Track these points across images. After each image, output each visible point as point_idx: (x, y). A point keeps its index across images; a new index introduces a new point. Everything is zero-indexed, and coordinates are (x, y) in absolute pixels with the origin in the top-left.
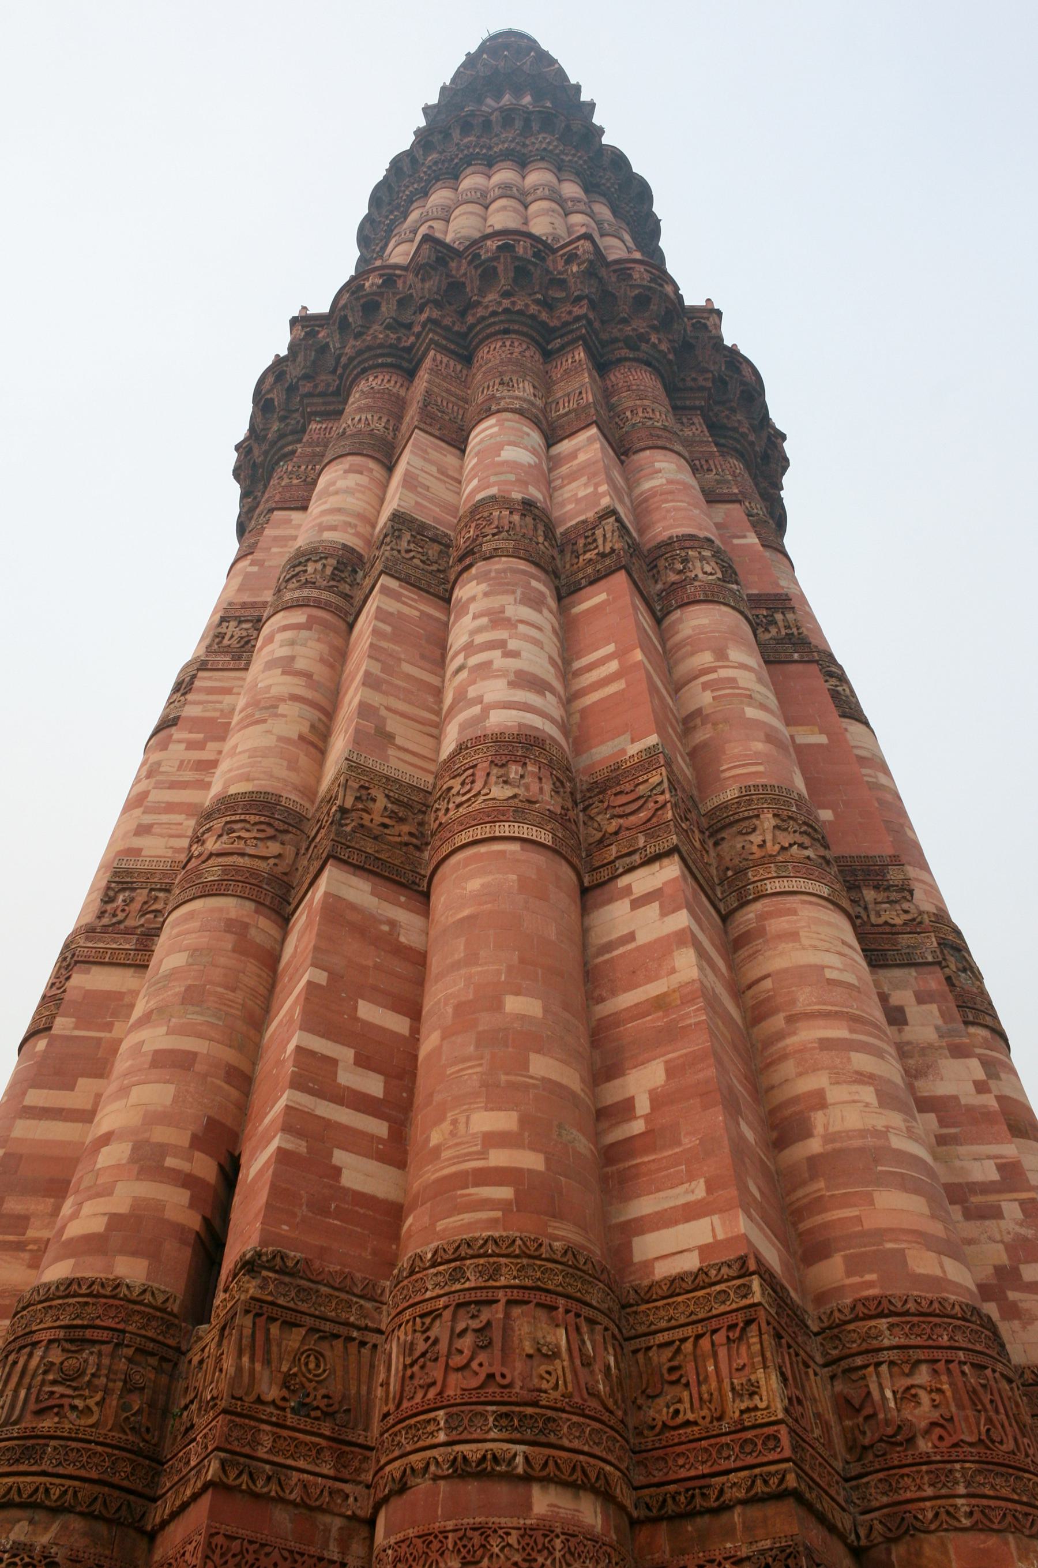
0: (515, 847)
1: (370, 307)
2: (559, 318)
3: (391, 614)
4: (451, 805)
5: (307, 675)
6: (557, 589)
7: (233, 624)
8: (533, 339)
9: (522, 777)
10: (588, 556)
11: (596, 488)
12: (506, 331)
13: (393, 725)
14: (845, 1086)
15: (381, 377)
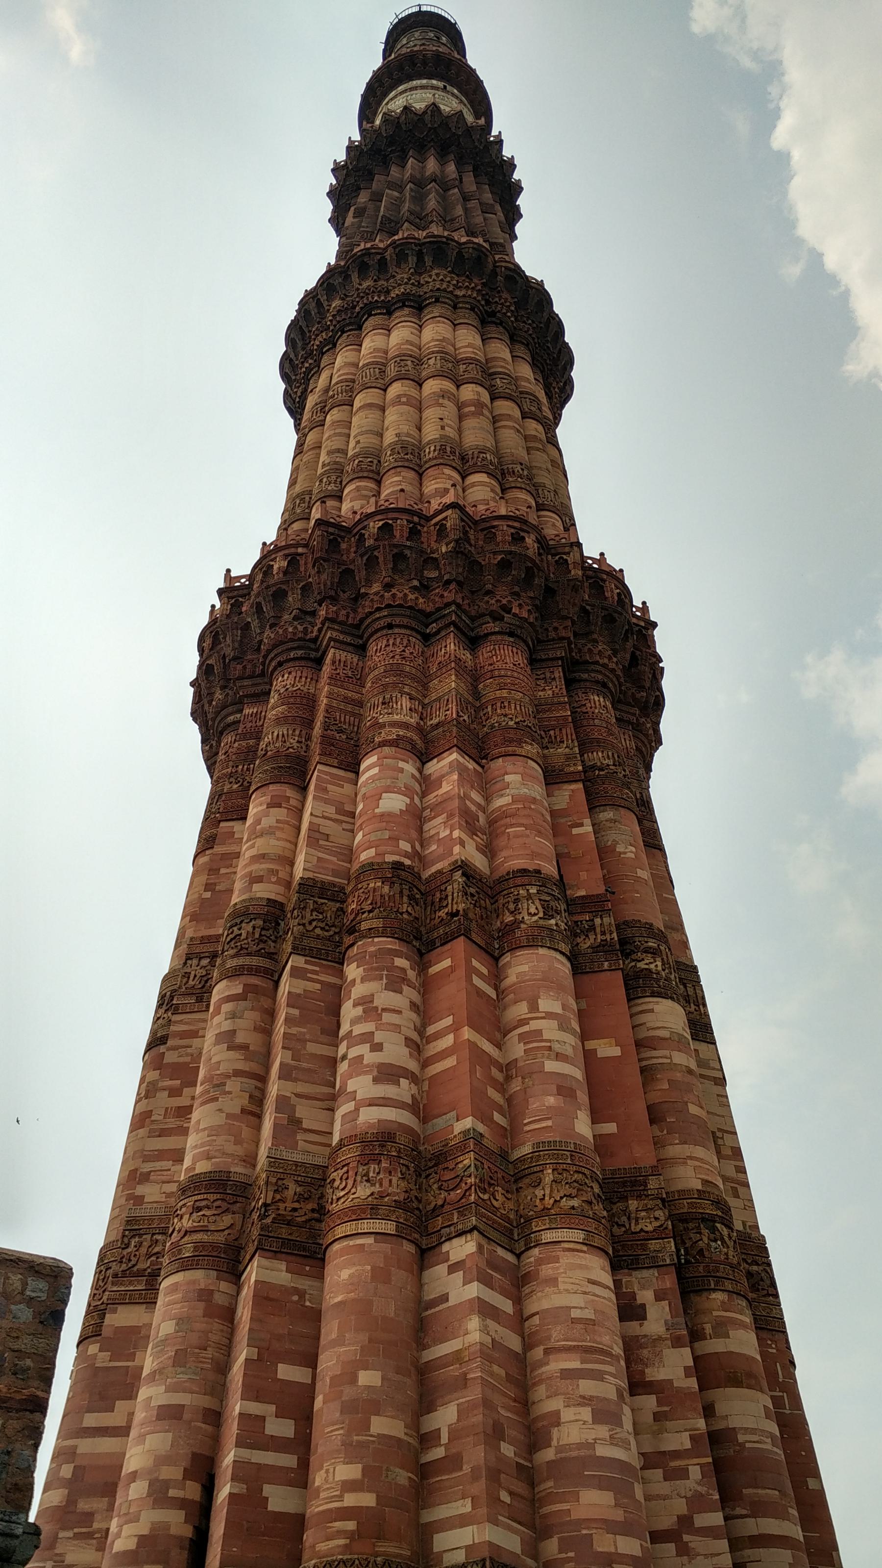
1: (279, 596)
2: (434, 602)
3: (299, 995)
4: (334, 1197)
6: (419, 950)
8: (412, 629)
9: (378, 1173)
11: (451, 832)
12: (390, 626)
13: (303, 1111)
14: (572, 1408)
15: (294, 674)
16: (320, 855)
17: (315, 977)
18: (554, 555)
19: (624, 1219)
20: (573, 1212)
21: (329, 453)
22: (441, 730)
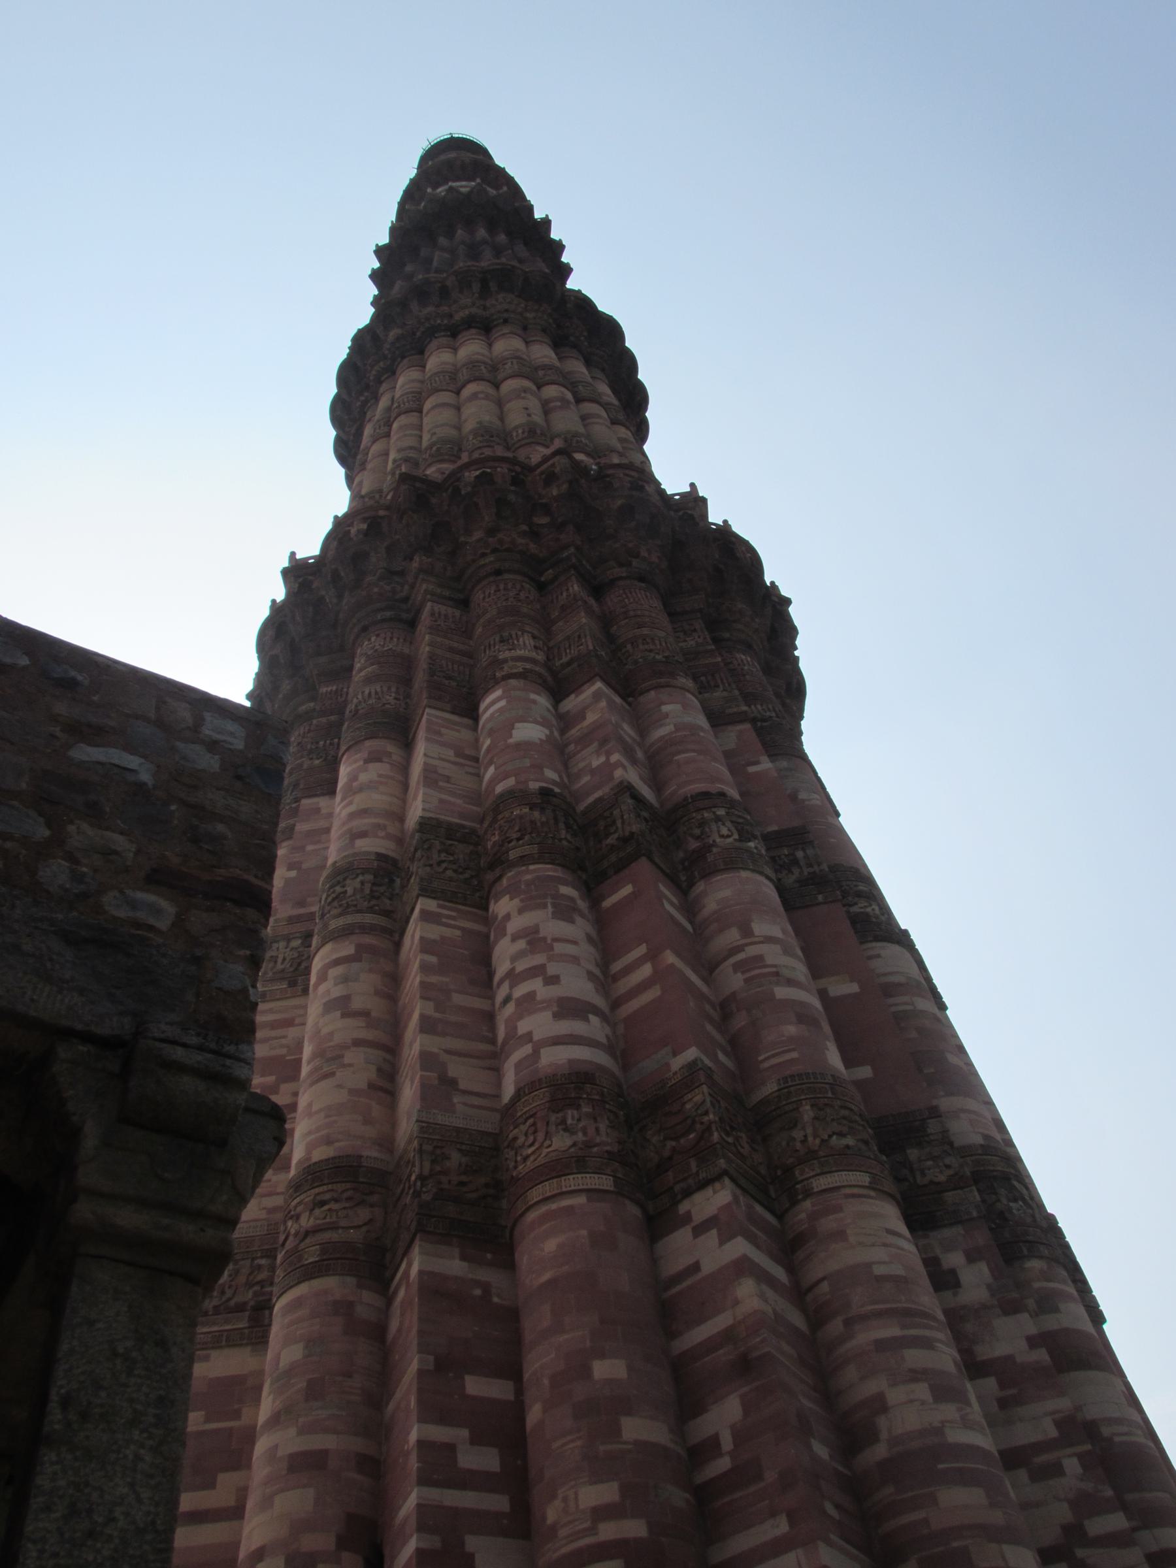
0: (581, 1200)
3: (434, 941)
4: (519, 1158)
5: (365, 1014)
9: (579, 1120)
10: (611, 840)
11: (608, 759)
12: (498, 572)
13: (455, 1069)
17: (453, 922)
18: (676, 511)
21: (399, 451)
22: (575, 665)
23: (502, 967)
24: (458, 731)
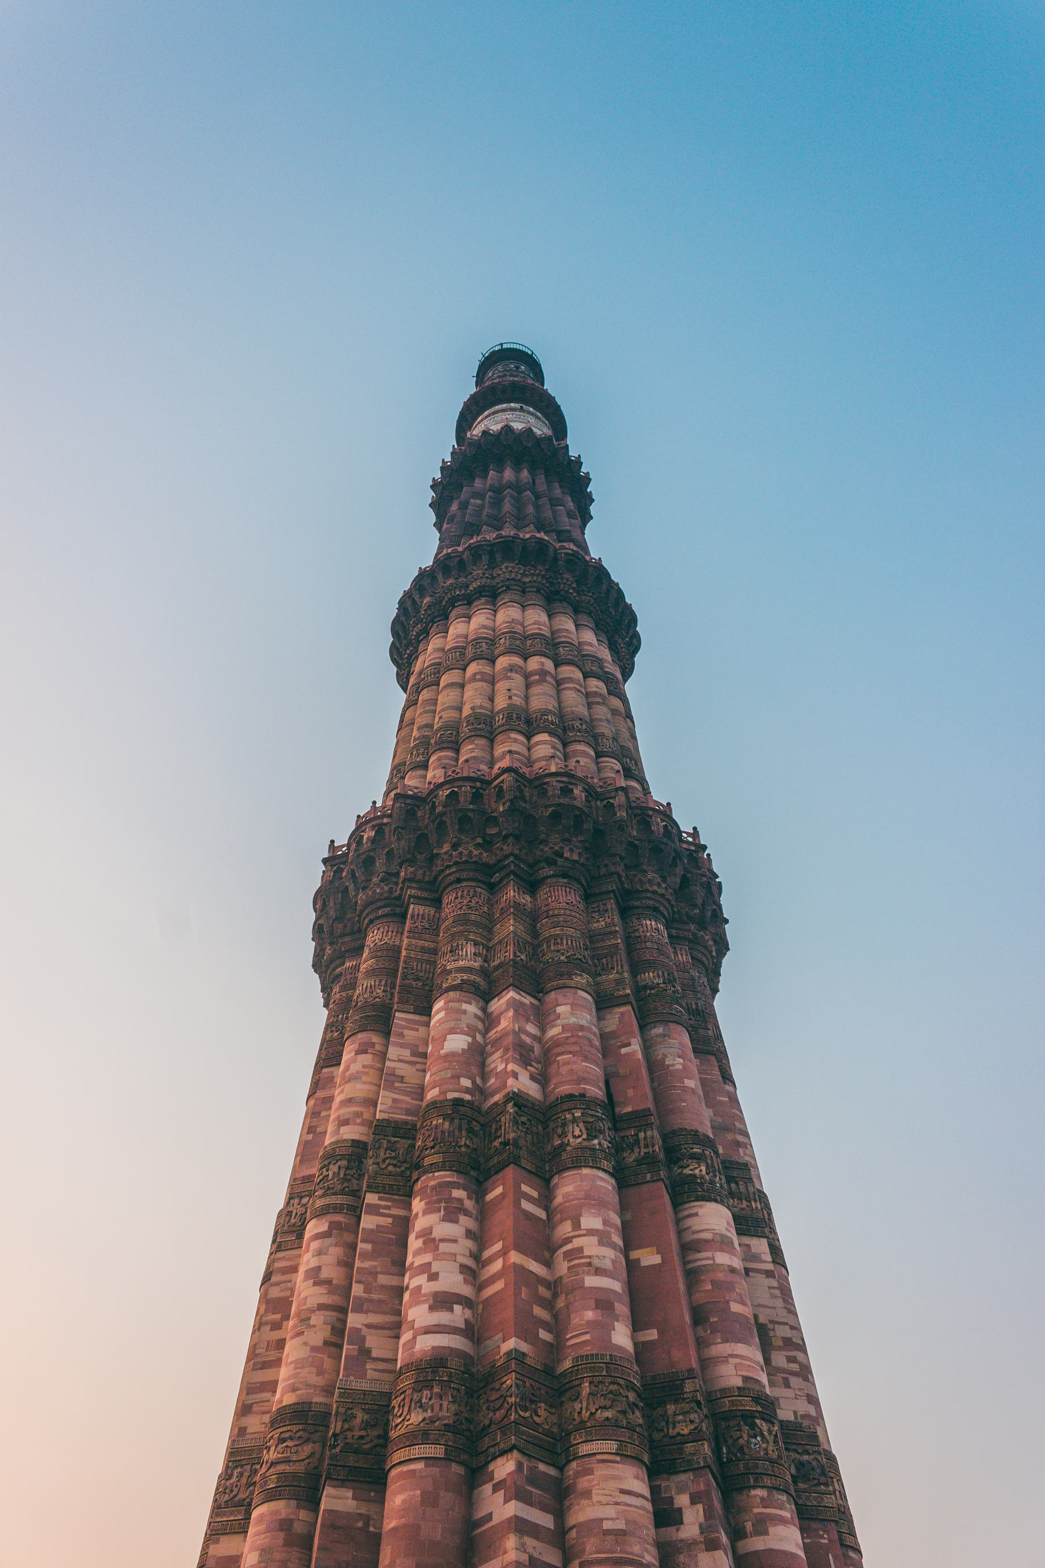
0: (419, 1466)
1: (368, 862)
2: (496, 855)
3: (372, 1230)
5: (328, 1282)
6: (477, 1180)
7: (296, 1201)
9: (430, 1399)
12: (459, 881)
15: (381, 930)
16: (397, 1096)
18: (602, 800)
19: (663, 1424)
20: (607, 1423)
21: (419, 728)
23: (409, 1260)
24: (417, 1030)
